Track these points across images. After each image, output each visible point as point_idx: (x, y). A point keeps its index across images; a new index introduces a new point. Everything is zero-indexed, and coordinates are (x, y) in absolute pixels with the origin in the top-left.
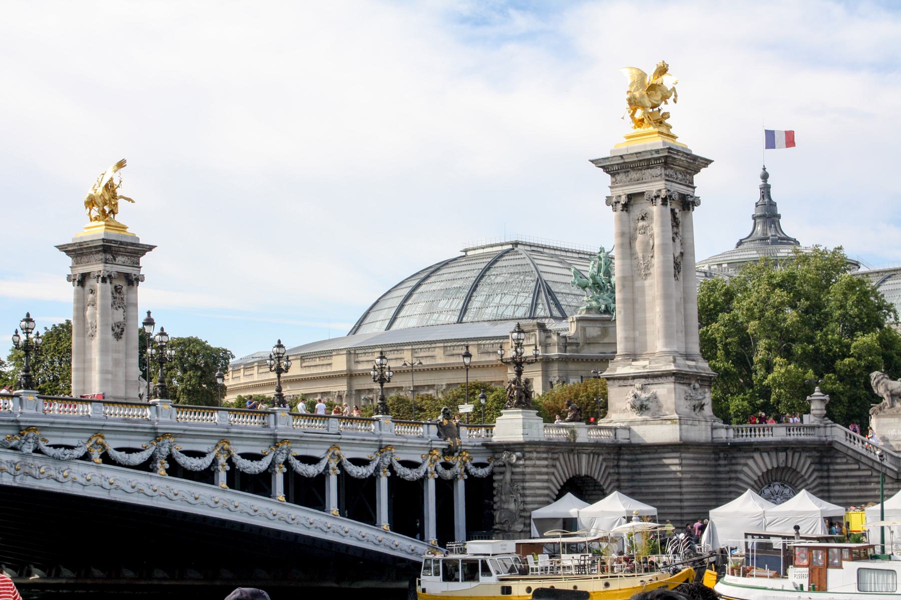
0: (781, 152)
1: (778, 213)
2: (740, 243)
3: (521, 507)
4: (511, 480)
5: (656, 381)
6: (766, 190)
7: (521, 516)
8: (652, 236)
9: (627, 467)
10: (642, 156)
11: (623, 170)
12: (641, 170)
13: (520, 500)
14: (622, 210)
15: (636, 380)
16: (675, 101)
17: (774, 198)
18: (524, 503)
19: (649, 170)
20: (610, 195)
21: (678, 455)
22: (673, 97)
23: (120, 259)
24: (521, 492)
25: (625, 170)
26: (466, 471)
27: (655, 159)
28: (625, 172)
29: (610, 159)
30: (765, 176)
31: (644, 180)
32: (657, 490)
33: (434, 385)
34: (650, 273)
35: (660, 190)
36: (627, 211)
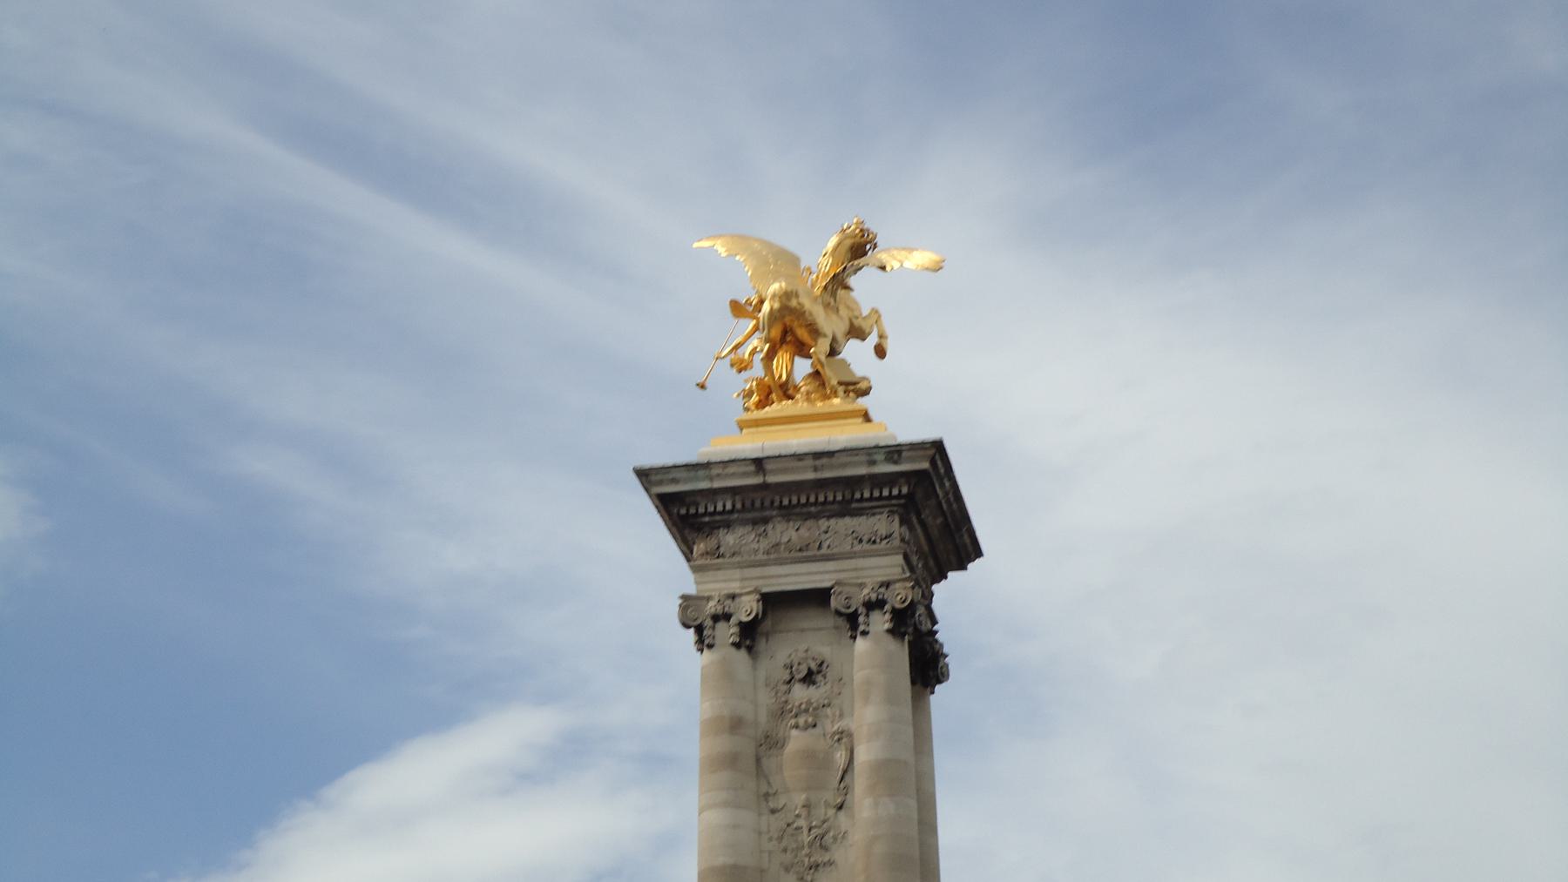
8: (845, 737)
10: (832, 467)
11: (750, 515)
12: (816, 517)
14: (737, 645)
16: (880, 352)
19: (847, 520)
20: (692, 590)
22: (872, 340)
25: (756, 514)
27: (877, 481)
28: (755, 522)
29: (715, 471)
31: (824, 551)
34: (830, 863)
35: (887, 585)
36: (750, 649)
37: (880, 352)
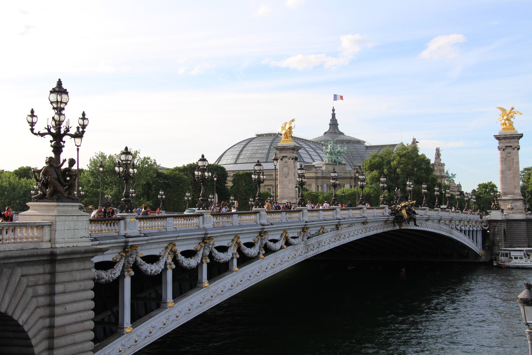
0: (339, 101)
1: (338, 123)
2: (325, 133)
3: (501, 238)
4: (497, 231)
5: (516, 201)
6: (334, 115)
7: (501, 241)
8: (513, 159)
9: (509, 226)
13: (500, 236)
15: (509, 201)
16: (514, 118)
17: (337, 117)
18: (501, 237)
21: (526, 223)
22: (513, 117)
23: (295, 152)
24: (501, 234)
26: (482, 227)
30: (333, 110)
32: (518, 233)
33: (272, 185)
34: (511, 170)
37: (514, 118)
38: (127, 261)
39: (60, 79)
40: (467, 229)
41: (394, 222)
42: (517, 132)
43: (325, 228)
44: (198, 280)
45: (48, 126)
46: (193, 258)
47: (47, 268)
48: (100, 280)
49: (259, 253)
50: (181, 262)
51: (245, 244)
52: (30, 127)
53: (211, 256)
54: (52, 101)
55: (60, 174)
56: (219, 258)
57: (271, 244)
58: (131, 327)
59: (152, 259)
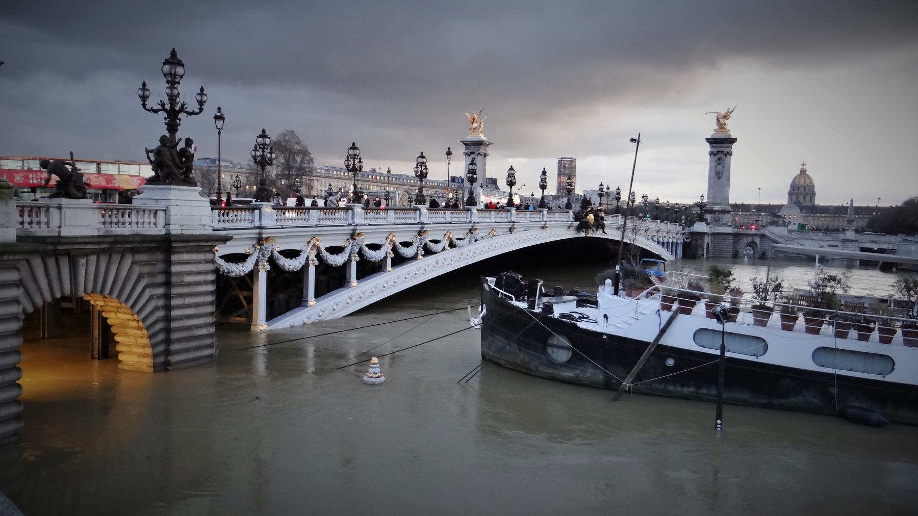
38: (262, 255)
39: (174, 49)
40: (666, 240)
41: (578, 229)
42: (731, 136)
43: (496, 230)
44: (346, 279)
45: (161, 101)
46: (340, 255)
47: (159, 256)
48: (229, 273)
49: (417, 254)
50: (326, 259)
51: (401, 243)
52: (142, 102)
53: (360, 253)
54: (166, 73)
55: (175, 153)
56: (369, 257)
57: (431, 245)
58: (267, 324)
59: (292, 254)
